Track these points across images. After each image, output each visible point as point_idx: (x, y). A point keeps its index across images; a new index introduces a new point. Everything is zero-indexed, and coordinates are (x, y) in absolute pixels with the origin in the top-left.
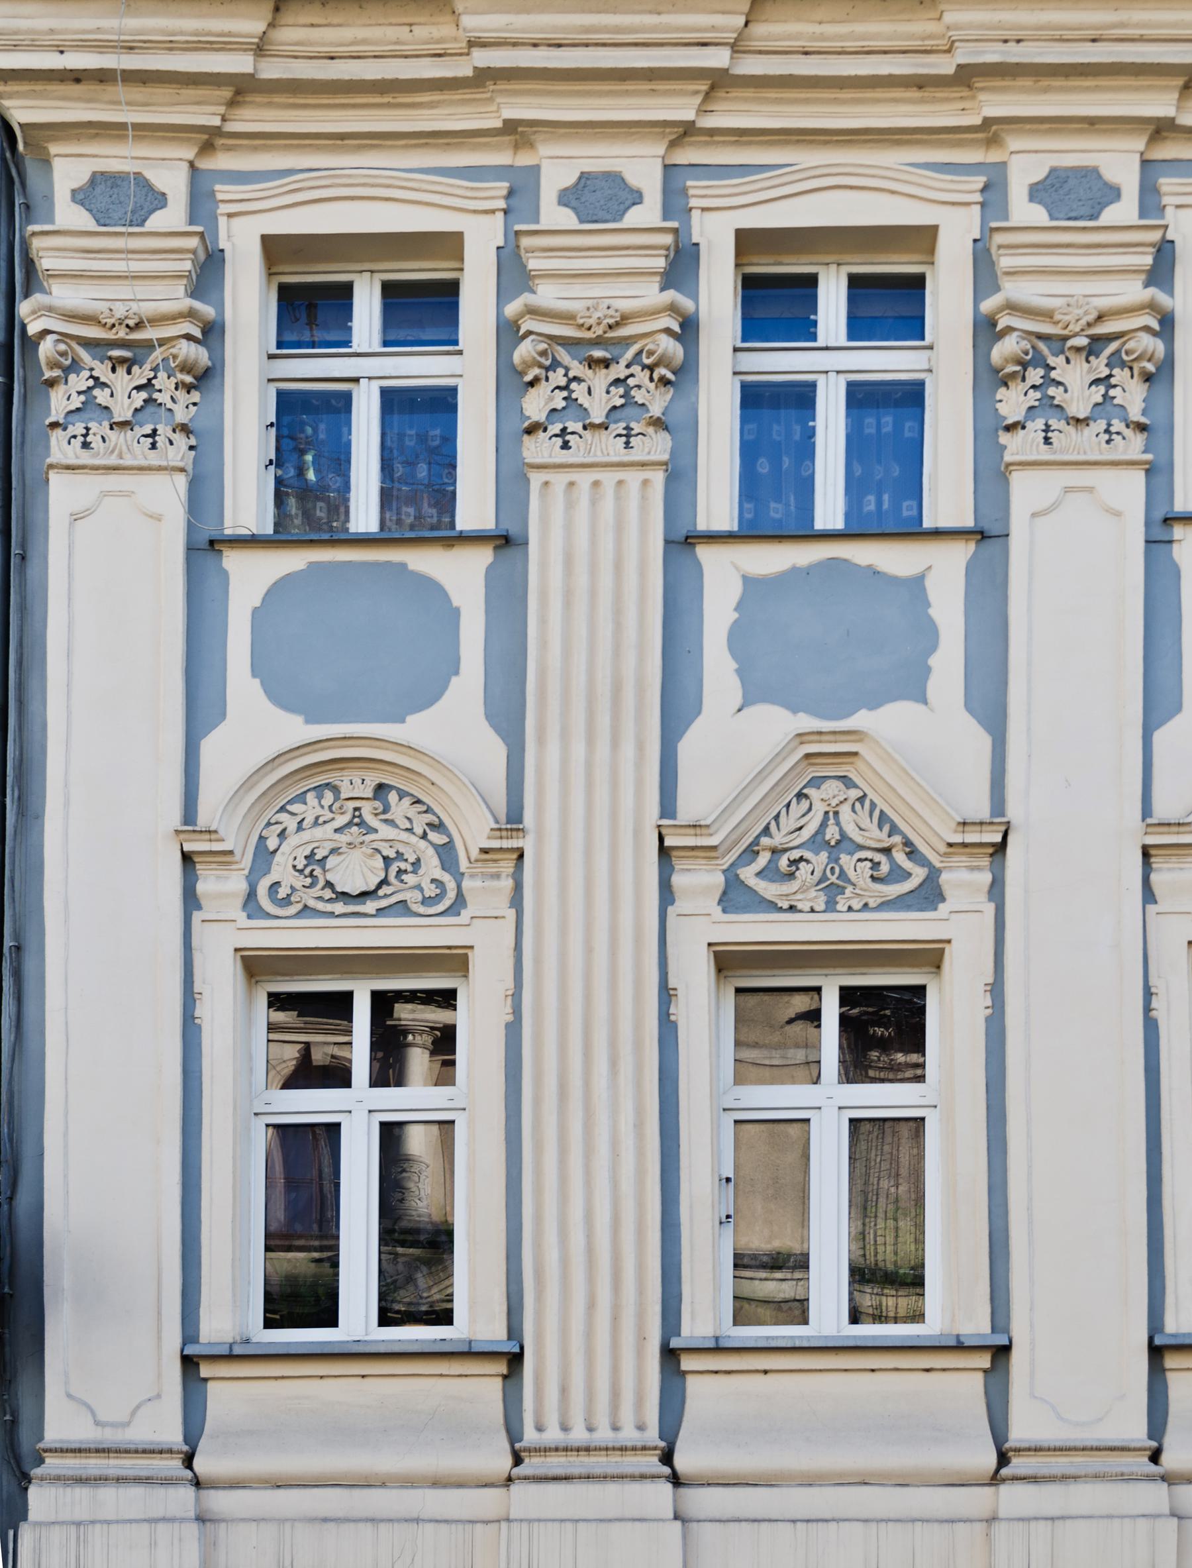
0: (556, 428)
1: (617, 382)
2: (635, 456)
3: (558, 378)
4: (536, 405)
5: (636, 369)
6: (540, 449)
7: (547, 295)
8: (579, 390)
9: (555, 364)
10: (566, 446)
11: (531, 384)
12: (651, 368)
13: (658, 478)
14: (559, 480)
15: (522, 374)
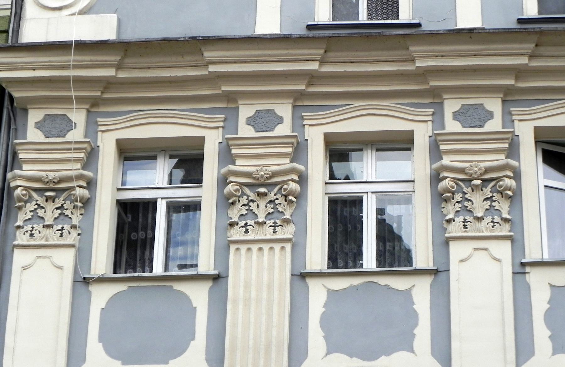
0: (242, 223)
1: (271, 202)
2: (278, 236)
3: (244, 200)
4: (234, 214)
5: (279, 196)
6: (237, 234)
7: (241, 165)
8: (253, 206)
9: (243, 194)
10: (247, 231)
11: (233, 203)
12: (286, 196)
13: (288, 246)
14: (243, 248)
15: (228, 199)
